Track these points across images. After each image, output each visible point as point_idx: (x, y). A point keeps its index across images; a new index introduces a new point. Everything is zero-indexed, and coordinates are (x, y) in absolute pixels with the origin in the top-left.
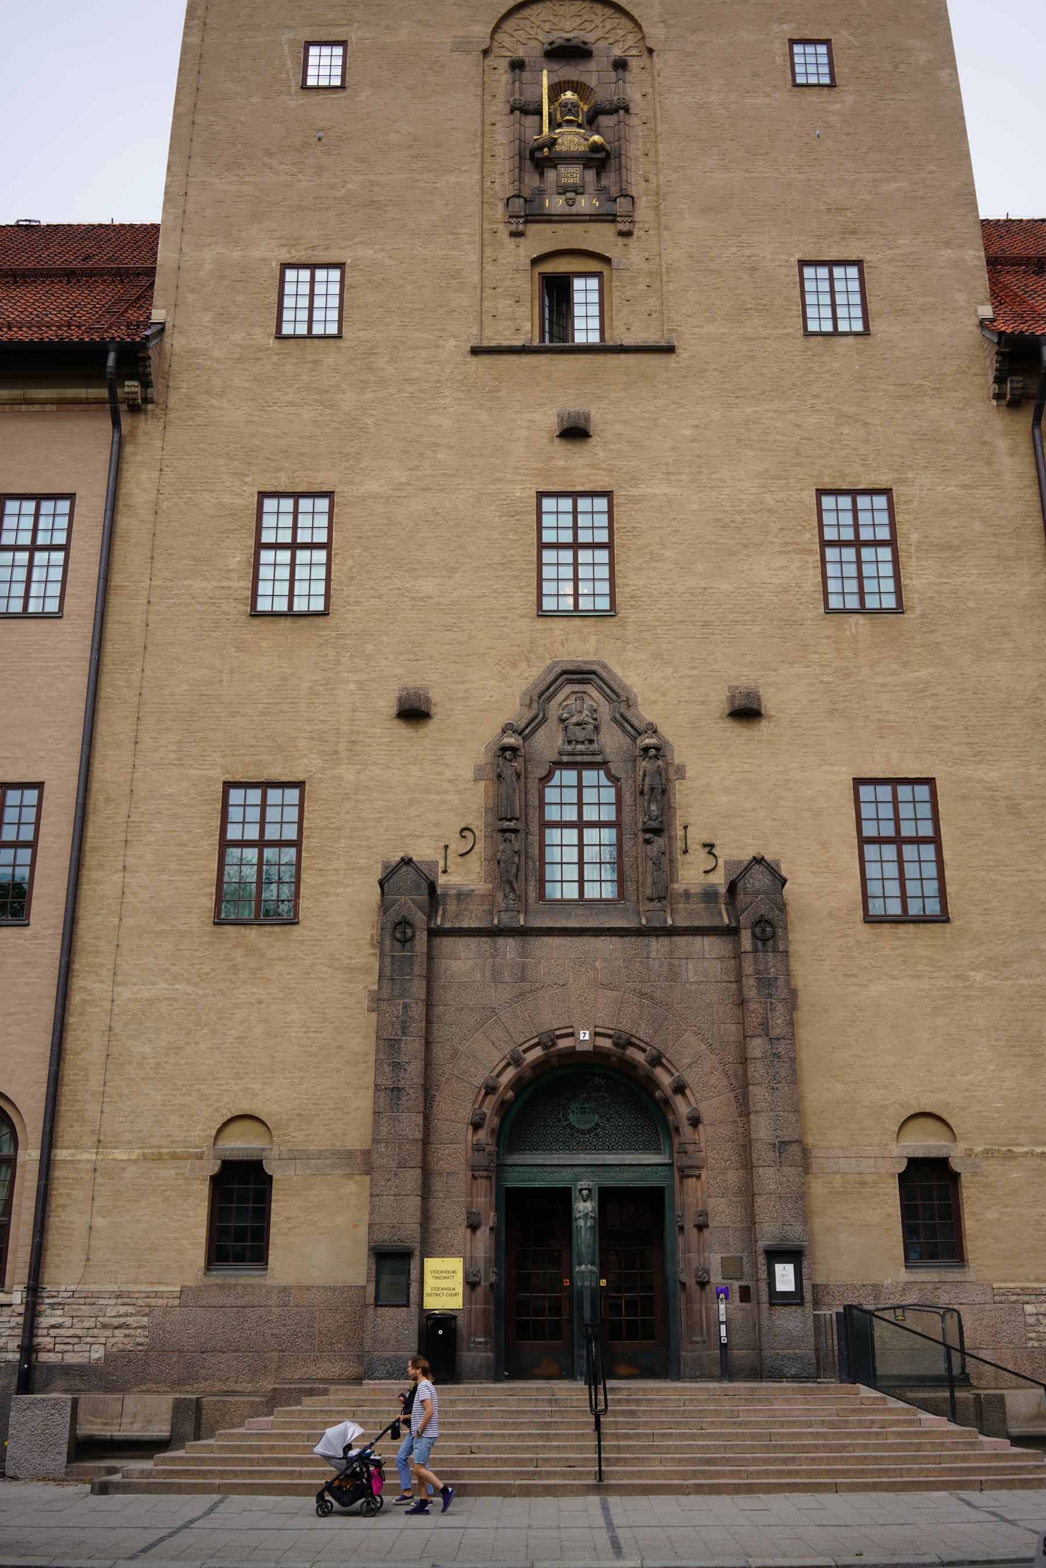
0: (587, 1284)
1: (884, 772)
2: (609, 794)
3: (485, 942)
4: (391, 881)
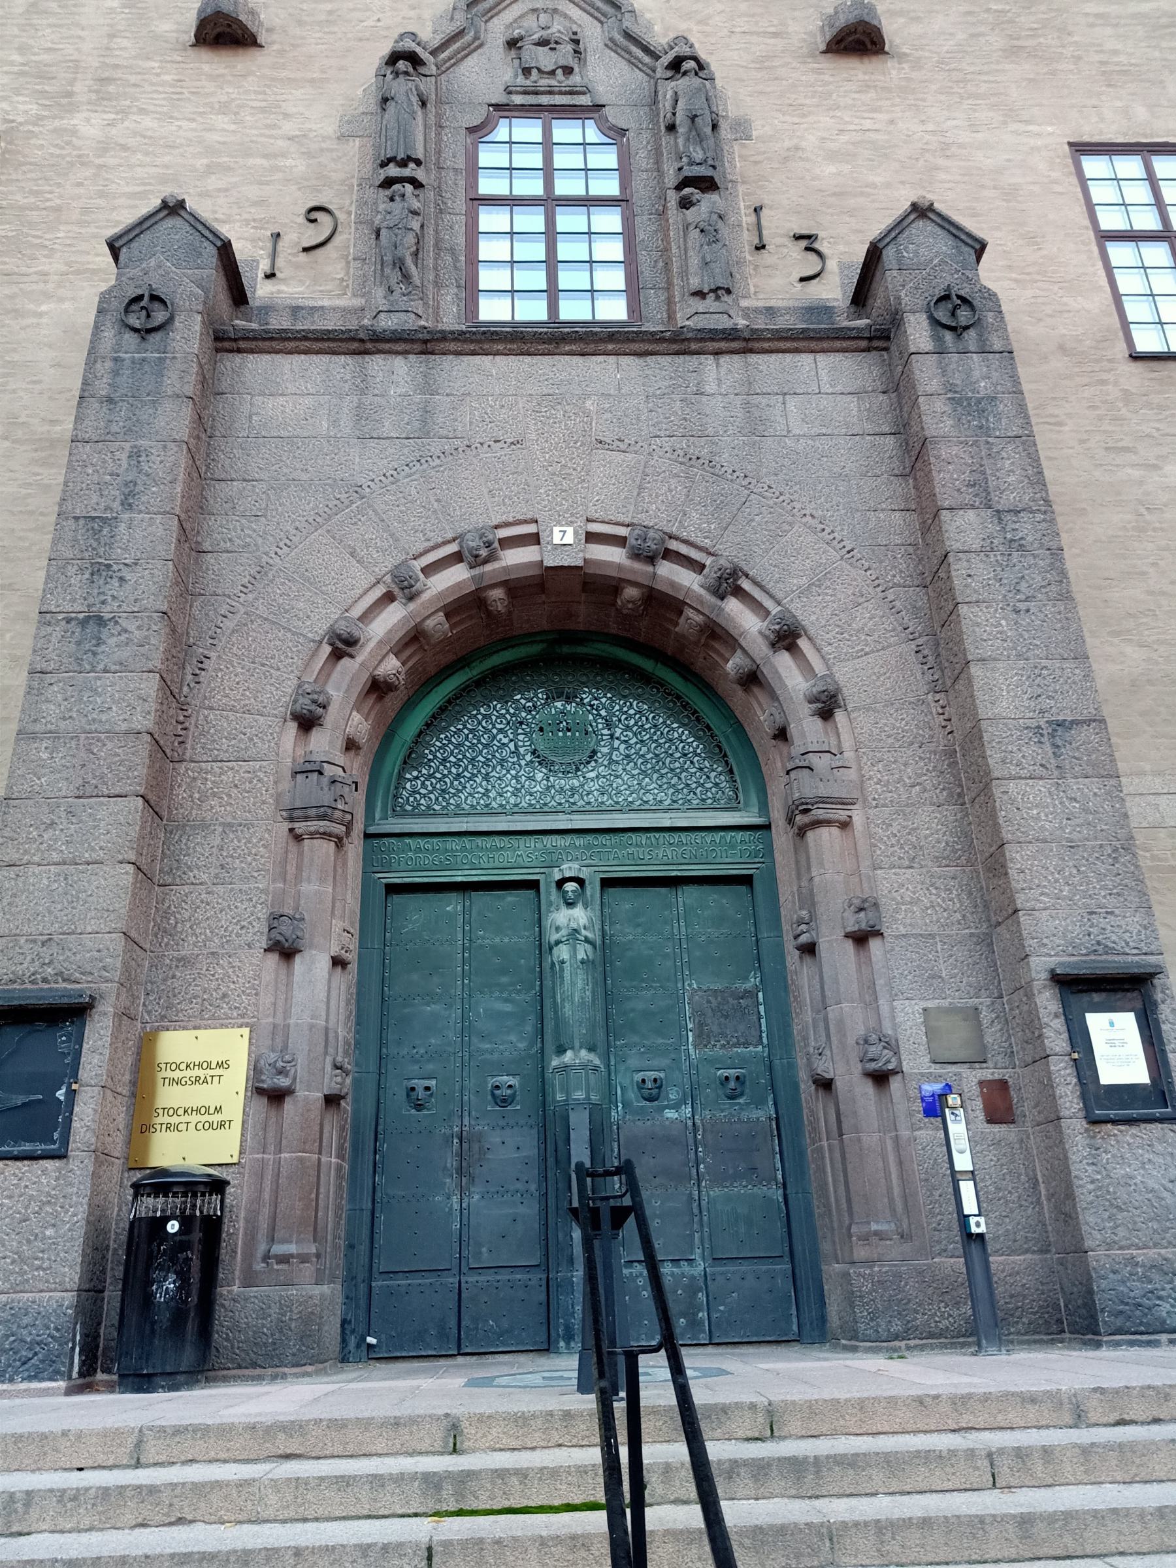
0: (579, 1095)
1: (1125, 134)
2: (609, 158)
3: (341, 366)
4: (134, 245)
